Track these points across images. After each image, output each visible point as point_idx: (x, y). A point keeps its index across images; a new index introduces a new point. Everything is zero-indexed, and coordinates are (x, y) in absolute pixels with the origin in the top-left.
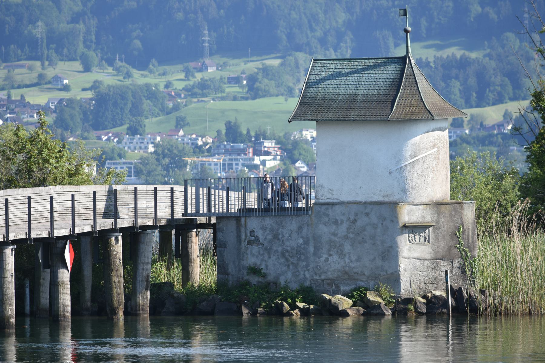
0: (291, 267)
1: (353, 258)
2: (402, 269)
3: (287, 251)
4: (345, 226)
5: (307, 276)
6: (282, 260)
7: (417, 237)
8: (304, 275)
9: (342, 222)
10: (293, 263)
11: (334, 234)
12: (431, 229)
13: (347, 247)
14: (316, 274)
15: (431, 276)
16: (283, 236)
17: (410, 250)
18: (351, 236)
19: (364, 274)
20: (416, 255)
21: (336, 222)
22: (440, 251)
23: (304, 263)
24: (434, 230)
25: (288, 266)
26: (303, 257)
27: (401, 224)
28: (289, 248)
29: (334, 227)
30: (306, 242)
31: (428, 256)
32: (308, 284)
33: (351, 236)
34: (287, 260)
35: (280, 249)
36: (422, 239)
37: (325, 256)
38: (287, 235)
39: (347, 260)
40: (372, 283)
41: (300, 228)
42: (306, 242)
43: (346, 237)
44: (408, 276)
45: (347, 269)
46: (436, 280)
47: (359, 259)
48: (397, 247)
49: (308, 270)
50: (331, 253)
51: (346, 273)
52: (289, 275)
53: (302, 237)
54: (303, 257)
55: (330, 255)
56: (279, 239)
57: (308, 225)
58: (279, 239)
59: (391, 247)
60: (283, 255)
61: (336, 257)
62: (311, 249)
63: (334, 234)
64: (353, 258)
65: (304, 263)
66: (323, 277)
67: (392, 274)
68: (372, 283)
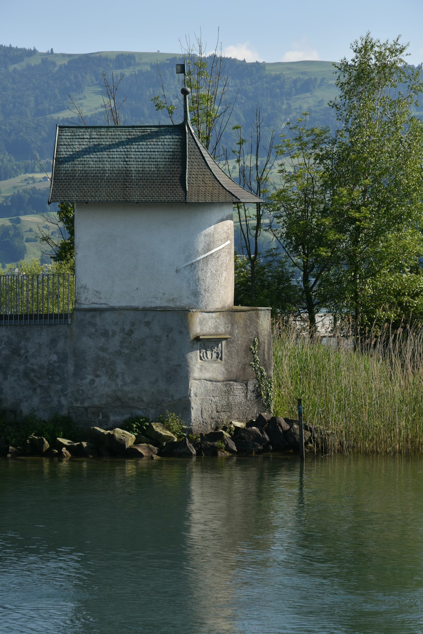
0: (38, 390)
1: (128, 380)
2: (192, 395)
3: (33, 370)
4: (116, 340)
5: (64, 402)
6: (25, 382)
7: (209, 353)
8: (59, 402)
9: (114, 333)
10: (41, 386)
11: (103, 349)
12: (224, 342)
13: (120, 366)
14: (77, 400)
15: (224, 402)
16: (27, 352)
17: (201, 370)
18: (126, 351)
19: (142, 401)
20: (208, 375)
21: (105, 334)
22: (234, 370)
23: (59, 387)
24: (227, 345)
25: (34, 390)
26: (57, 379)
27: (192, 337)
28: (35, 367)
29: (103, 340)
30: (63, 359)
31: (221, 377)
32: (64, 412)
33: (126, 351)
34: (32, 382)
35: (22, 368)
36: (215, 355)
37: (90, 377)
38: (33, 350)
39: (120, 382)
40: (152, 411)
41: (53, 342)
42: (63, 359)
43: (119, 353)
44: (199, 402)
45: (119, 394)
46: (229, 407)
47: (136, 381)
48: (188, 366)
49: (65, 396)
50: (99, 373)
51: (118, 399)
52: (36, 401)
53: (56, 353)
54: (57, 379)
55: (97, 376)
56: (20, 355)
57: (66, 337)
58: (20, 355)
59: (179, 365)
60: (26, 375)
61: (104, 379)
62: (71, 368)
63: (103, 349)
64: (128, 380)
65: (59, 387)
66: (86, 404)
67: (180, 400)
68: (152, 411)
